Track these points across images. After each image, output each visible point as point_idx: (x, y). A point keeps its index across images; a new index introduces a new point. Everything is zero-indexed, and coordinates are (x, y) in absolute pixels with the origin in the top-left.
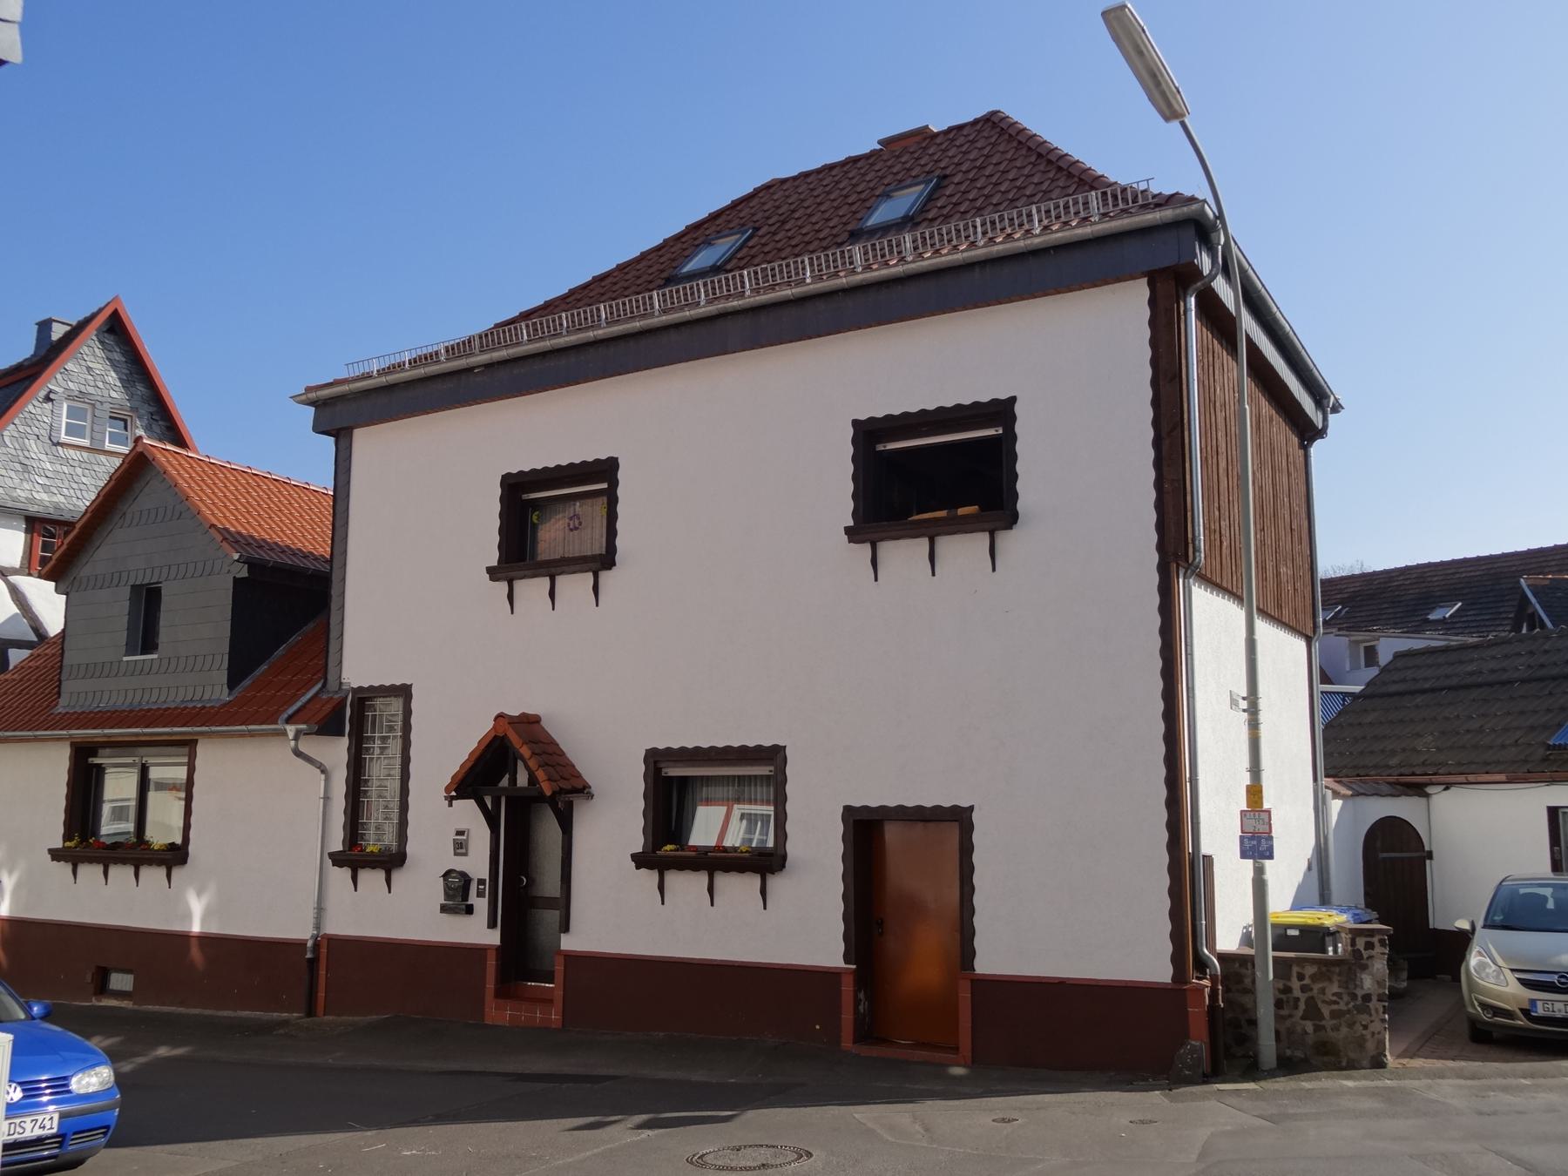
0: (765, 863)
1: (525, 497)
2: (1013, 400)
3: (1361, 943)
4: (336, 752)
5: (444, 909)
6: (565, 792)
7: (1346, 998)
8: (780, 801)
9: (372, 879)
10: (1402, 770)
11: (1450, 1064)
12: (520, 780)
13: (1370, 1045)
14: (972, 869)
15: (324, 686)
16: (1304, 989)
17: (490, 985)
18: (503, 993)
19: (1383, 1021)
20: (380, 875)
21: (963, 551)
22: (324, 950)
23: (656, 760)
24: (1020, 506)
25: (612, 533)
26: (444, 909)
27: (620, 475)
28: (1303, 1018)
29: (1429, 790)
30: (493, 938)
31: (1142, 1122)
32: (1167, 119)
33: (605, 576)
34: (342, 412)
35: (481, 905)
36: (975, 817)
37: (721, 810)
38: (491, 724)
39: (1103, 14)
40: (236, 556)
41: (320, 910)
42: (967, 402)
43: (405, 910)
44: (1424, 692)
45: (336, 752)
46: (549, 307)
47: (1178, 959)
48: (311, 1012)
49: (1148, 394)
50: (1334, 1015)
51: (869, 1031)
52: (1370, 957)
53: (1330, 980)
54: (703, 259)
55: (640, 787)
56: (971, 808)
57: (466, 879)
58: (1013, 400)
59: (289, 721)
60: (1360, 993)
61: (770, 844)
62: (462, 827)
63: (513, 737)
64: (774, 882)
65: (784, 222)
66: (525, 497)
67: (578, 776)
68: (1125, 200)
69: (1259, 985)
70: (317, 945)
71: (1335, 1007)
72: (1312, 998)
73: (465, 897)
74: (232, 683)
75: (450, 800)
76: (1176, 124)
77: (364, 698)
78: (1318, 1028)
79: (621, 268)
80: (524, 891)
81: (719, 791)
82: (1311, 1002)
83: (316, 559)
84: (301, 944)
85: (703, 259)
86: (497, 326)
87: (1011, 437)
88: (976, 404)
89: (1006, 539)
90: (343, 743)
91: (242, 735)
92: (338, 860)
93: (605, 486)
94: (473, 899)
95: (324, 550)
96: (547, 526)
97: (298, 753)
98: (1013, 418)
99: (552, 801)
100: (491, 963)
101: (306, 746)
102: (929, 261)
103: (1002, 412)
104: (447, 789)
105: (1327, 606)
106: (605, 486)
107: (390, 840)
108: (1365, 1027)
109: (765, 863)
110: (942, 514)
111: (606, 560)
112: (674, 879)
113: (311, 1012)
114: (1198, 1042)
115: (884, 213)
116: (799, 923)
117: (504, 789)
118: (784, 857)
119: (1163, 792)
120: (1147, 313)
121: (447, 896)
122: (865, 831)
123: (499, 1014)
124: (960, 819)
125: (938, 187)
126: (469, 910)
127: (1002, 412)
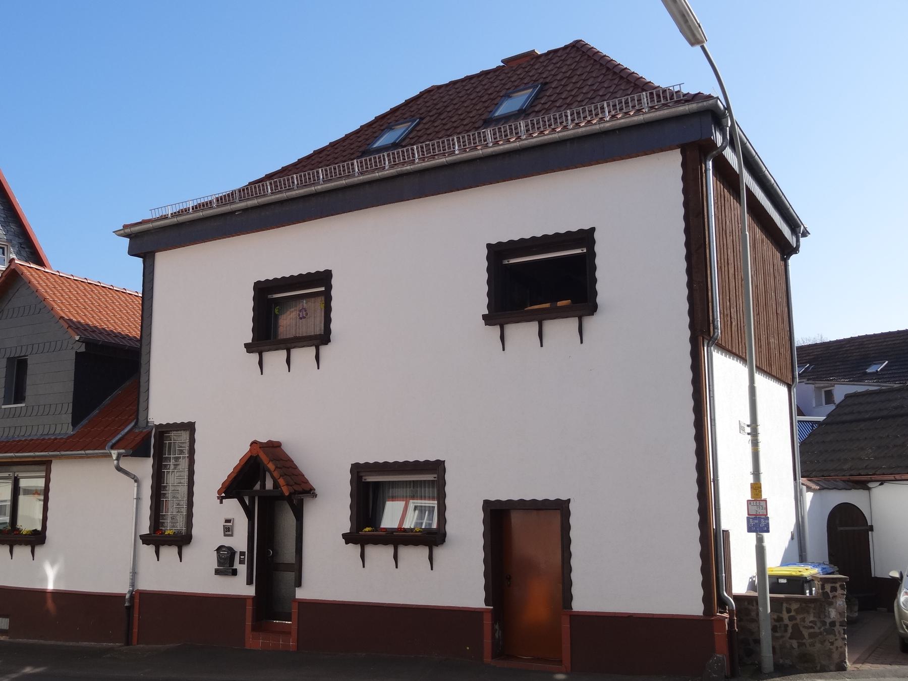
1: (270, 296)
3: (828, 588)
4: (144, 468)
5: (217, 572)
6: (298, 492)
7: (819, 624)
8: (441, 497)
9: (169, 553)
11: (888, 667)
12: (268, 485)
13: (836, 656)
14: (569, 541)
15: (136, 423)
16: (791, 618)
17: (249, 623)
18: (255, 628)
19: (844, 639)
20: (174, 550)
21: (561, 330)
22: (137, 601)
23: (358, 471)
24: (599, 300)
25: (328, 320)
26: (217, 572)
27: (333, 282)
28: (790, 638)
29: (870, 485)
30: (251, 591)
32: (692, 44)
33: (324, 349)
34: (147, 241)
35: (242, 569)
37: (401, 504)
38: (247, 448)
40: (77, 338)
41: (134, 574)
42: (563, 231)
43: (191, 573)
44: (864, 420)
45: (144, 468)
46: (285, 171)
47: (707, 600)
48: (128, 642)
49: (682, 225)
50: (812, 635)
51: (502, 651)
52: (834, 597)
53: (808, 612)
54: (386, 139)
55: (347, 489)
56: (569, 500)
57: (231, 552)
59: (112, 447)
60: (828, 621)
61: (435, 526)
62: (229, 517)
63: (264, 458)
64: (438, 552)
65: (440, 114)
66: (270, 296)
67: (306, 482)
68: (665, 98)
69: (762, 617)
70: (132, 597)
71: (812, 630)
72: (797, 624)
73: (232, 564)
74: (75, 423)
75: (221, 499)
77: (164, 431)
78: (801, 645)
79: (333, 145)
80: (272, 558)
81: (399, 491)
82: (796, 628)
83: (131, 339)
84: (121, 597)
85: (386, 139)
86: (250, 184)
87: (592, 254)
89: (590, 323)
90: (150, 461)
91: (81, 457)
92: (146, 539)
93: (323, 289)
94: (237, 565)
95: (136, 333)
96: (287, 316)
97: (119, 469)
98: (593, 242)
100: (249, 608)
101: (126, 464)
102: (536, 139)
103: (586, 237)
104: (219, 492)
105: (801, 364)
106: (323, 289)
107: (181, 525)
108: (832, 643)
109: (432, 539)
110: (547, 305)
111: (323, 338)
112: (372, 551)
113: (128, 642)
115: (507, 107)
116: (456, 579)
117: (257, 491)
118: (445, 535)
119: (695, 489)
120: (680, 172)
121: (219, 563)
122: (498, 515)
123: (255, 642)
124: (561, 508)
126: (234, 573)
127: (586, 237)
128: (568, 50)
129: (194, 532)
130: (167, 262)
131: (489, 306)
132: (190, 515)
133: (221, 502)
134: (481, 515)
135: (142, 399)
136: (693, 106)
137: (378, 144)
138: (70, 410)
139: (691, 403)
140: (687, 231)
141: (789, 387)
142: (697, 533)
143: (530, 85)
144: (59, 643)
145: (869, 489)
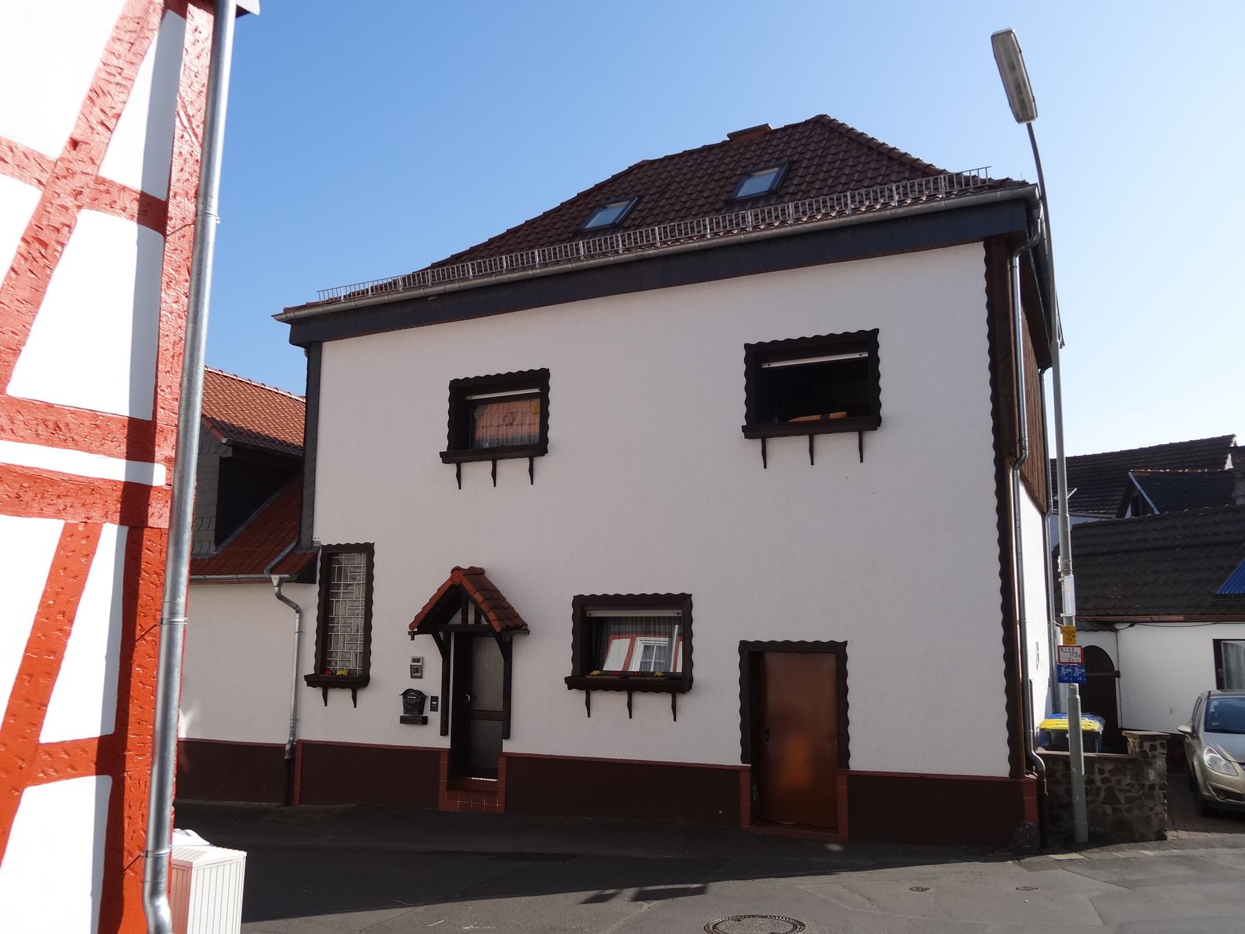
0: (676, 685)
1: (468, 398)
2: (876, 331)
3: (1147, 746)
4: (309, 596)
5: (403, 720)
6: (510, 628)
7: (1137, 787)
8: (687, 636)
9: (340, 697)
10: (1099, 612)
11: (1217, 836)
12: (470, 618)
13: (1155, 822)
14: (845, 690)
15: (298, 543)
16: (1104, 781)
17: (443, 780)
18: (451, 786)
19: (1163, 804)
20: (347, 694)
21: (837, 448)
22: (299, 753)
23: (582, 604)
24: (883, 412)
25: (544, 427)
26: (403, 720)
27: (552, 382)
28: (1104, 803)
29: (1118, 626)
30: (445, 743)
31: (1026, 888)
32: (1019, 120)
33: (539, 462)
34: (313, 328)
35: (435, 717)
36: (848, 650)
37: (625, 643)
38: (447, 576)
39: (993, 37)
40: (224, 440)
41: (295, 721)
42: (839, 332)
43: (369, 720)
44: (1103, 554)
45: (309, 596)
46: (474, 253)
47: (1012, 759)
48: (288, 801)
49: (985, 329)
50: (1130, 800)
51: (761, 815)
52: (1154, 756)
53: (1125, 774)
54: (601, 219)
55: (569, 625)
56: (846, 643)
57: (421, 697)
58: (876, 331)
59: (272, 571)
60: (1147, 783)
61: (679, 670)
62: (418, 655)
63: (468, 586)
64: (683, 700)
65: (663, 193)
66: (468, 398)
67: (517, 616)
68: (960, 183)
69: (1074, 778)
70: (293, 748)
71: (1129, 794)
72: (1110, 787)
73: (421, 711)
74: (218, 542)
75: (413, 635)
76: (1024, 126)
77: (333, 552)
78: (1115, 811)
79: (529, 223)
80: (473, 706)
81: (629, 628)
82: (1109, 791)
83: (296, 447)
84: (280, 748)
85: (601, 219)
86: (434, 266)
87: (874, 360)
88: (817, 338)
89: (872, 438)
90: (315, 588)
91: (230, 582)
92: (311, 681)
93: (537, 391)
94: (427, 712)
95: (298, 440)
96: (490, 423)
97: (280, 597)
98: (877, 345)
99: (498, 637)
100: (444, 762)
101: (287, 591)
102: (806, 225)
103: (868, 340)
104: (411, 626)
105: (1069, 491)
106: (537, 391)
107: (354, 665)
108: (1151, 809)
109: (676, 685)
110: (817, 417)
111: (536, 448)
112: (599, 698)
113: (288, 801)
114: (1031, 823)
115: (749, 188)
116: (705, 731)
117: (456, 626)
118: (691, 680)
119: (1000, 632)
120: (983, 268)
121: (406, 709)
122: (754, 656)
123: (450, 802)
124: (837, 651)
125: (789, 170)
126: (425, 721)
127: (868, 340)
128: (811, 126)
129: (372, 672)
130: (339, 355)
131: (747, 417)
132: (367, 653)
133: (413, 639)
134: (737, 658)
135: (305, 515)
136: (999, 194)
137: (593, 223)
138: (213, 525)
139: (996, 534)
140: (991, 336)
141: (1043, 514)
142: (1002, 682)
143: (772, 163)
144: (198, 802)
145: (1116, 631)
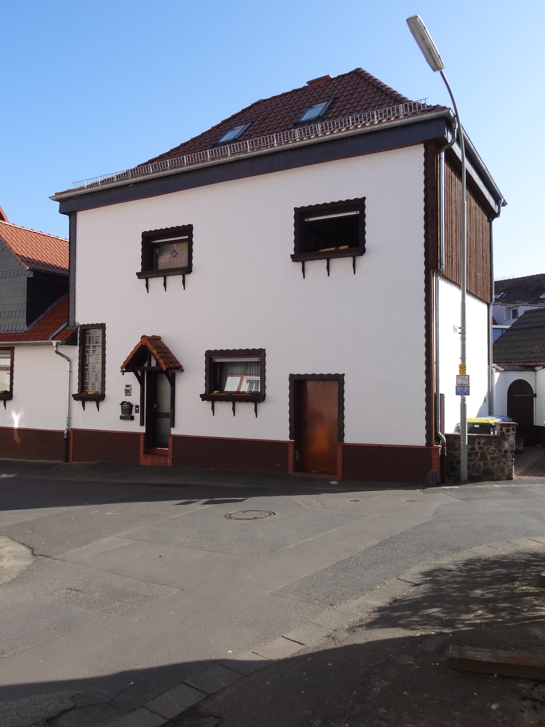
0: (257, 398)
1: (152, 242)
2: (364, 198)
3: (504, 429)
4: (74, 352)
5: (121, 418)
6: (172, 368)
7: (497, 452)
9: (91, 406)
10: (525, 360)
11: (539, 478)
12: (153, 363)
13: (506, 471)
15: (68, 324)
16: (480, 448)
17: (142, 449)
18: (145, 453)
20: (94, 404)
21: (341, 265)
22: (71, 435)
23: (210, 355)
24: (367, 245)
25: (190, 258)
26: (121, 418)
27: (194, 232)
29: (536, 368)
30: (143, 430)
31: (411, 501)
33: (188, 277)
34: (73, 204)
35: (137, 416)
36: (345, 378)
39: (407, 20)
40: (28, 268)
41: (69, 418)
43: (105, 418)
44: (535, 327)
45: (74, 352)
46: (162, 157)
48: (67, 460)
49: (423, 195)
50: (492, 459)
51: (300, 467)
52: (508, 435)
53: (491, 445)
54: (229, 136)
55: (204, 366)
56: (344, 375)
57: (130, 405)
58: (364, 198)
60: (503, 450)
61: (259, 391)
62: (128, 384)
63: (150, 346)
64: (260, 406)
65: (265, 119)
66: (152, 242)
67: (177, 362)
68: (415, 108)
69: (462, 447)
70: (68, 433)
71: (493, 456)
73: (130, 412)
74: (28, 323)
75: (123, 372)
76: (438, 73)
77: (86, 329)
78: (485, 464)
79: (193, 140)
80: (156, 409)
82: (483, 454)
83: (62, 269)
84: (62, 433)
85: (229, 136)
86: (138, 166)
87: (363, 215)
88: (348, 201)
89: (361, 261)
90: (77, 348)
91: (33, 345)
92: (76, 397)
93: (187, 237)
94: (133, 413)
95: (66, 265)
96: (164, 255)
97: (57, 352)
98: (364, 207)
99: (166, 373)
100: (142, 440)
101: (61, 349)
102: (328, 136)
103: (359, 204)
104: (122, 368)
106: (187, 237)
107: (98, 389)
108: (505, 464)
109: (257, 398)
110: (333, 249)
111: (187, 270)
112: (219, 405)
113: (67, 460)
114: (436, 470)
116: (271, 423)
117: (146, 367)
118: (265, 395)
119: (424, 368)
120: (423, 160)
121: (123, 412)
122: (299, 384)
123: (145, 460)
125: (333, 103)
126: (132, 418)
127: (359, 204)
128: (351, 76)
129: (107, 393)
131: (295, 249)
133: (123, 374)
136: (433, 114)
138: (25, 315)
141: (488, 305)
142: (424, 395)
143: (325, 99)
145: (535, 371)
